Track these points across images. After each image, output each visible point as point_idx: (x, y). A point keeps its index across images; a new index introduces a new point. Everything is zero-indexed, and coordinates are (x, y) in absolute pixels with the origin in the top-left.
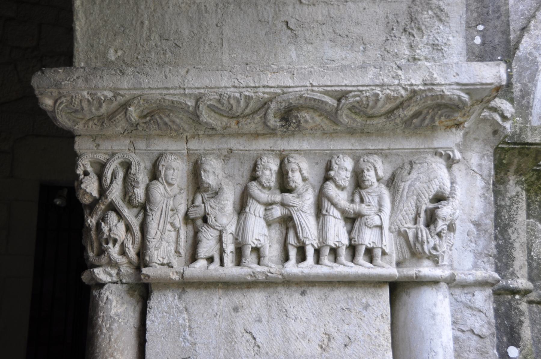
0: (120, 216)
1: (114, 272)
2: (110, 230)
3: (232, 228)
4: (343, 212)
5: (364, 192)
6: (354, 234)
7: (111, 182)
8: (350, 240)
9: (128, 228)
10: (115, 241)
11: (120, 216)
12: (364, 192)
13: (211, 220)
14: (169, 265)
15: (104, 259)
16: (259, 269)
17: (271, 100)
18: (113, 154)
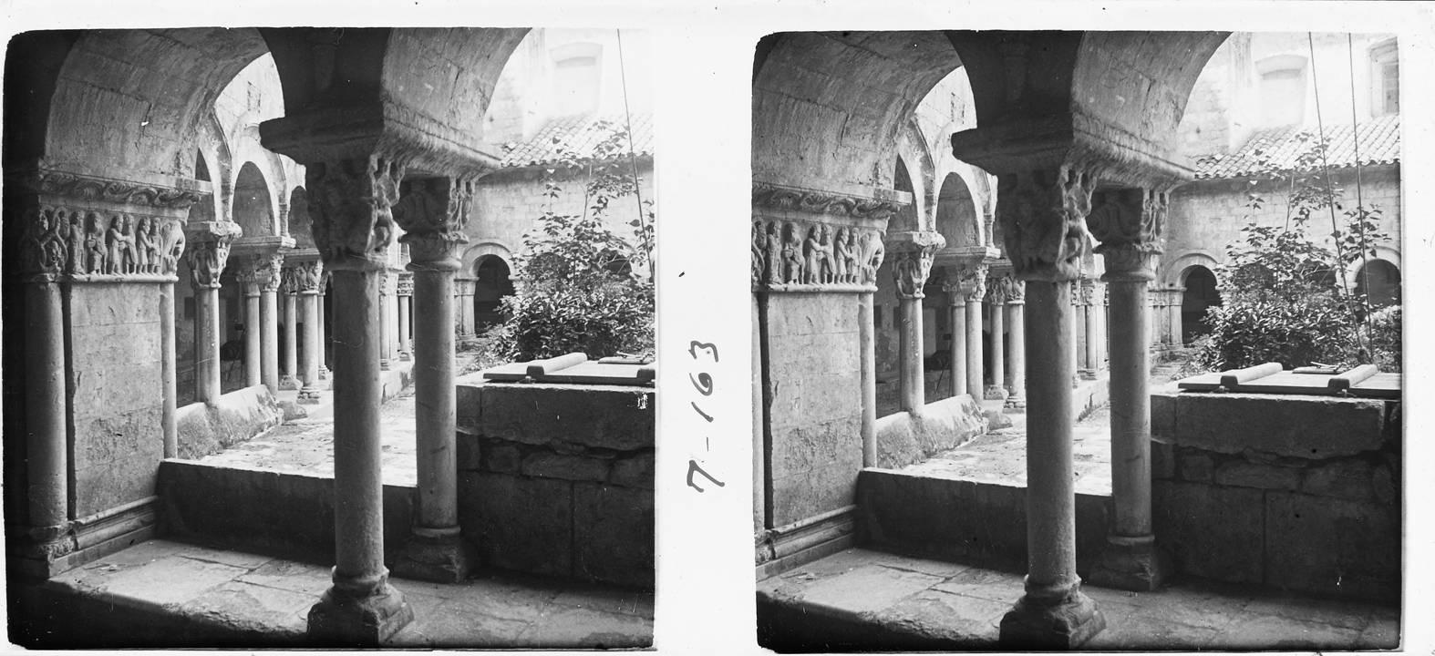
0: (60, 244)
1: (53, 276)
2: (57, 252)
3: (107, 253)
4: (147, 247)
5: (154, 237)
6: (151, 259)
7: (56, 225)
8: (149, 261)
9: (63, 252)
10: (58, 258)
11: (60, 244)
12: (154, 237)
13: (99, 248)
14: (81, 273)
15: (51, 268)
16: (120, 276)
17: (133, 189)
18: (57, 207)
